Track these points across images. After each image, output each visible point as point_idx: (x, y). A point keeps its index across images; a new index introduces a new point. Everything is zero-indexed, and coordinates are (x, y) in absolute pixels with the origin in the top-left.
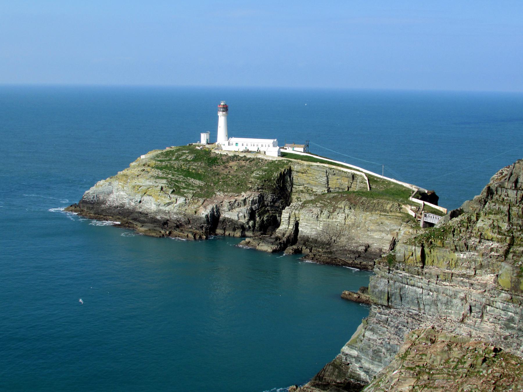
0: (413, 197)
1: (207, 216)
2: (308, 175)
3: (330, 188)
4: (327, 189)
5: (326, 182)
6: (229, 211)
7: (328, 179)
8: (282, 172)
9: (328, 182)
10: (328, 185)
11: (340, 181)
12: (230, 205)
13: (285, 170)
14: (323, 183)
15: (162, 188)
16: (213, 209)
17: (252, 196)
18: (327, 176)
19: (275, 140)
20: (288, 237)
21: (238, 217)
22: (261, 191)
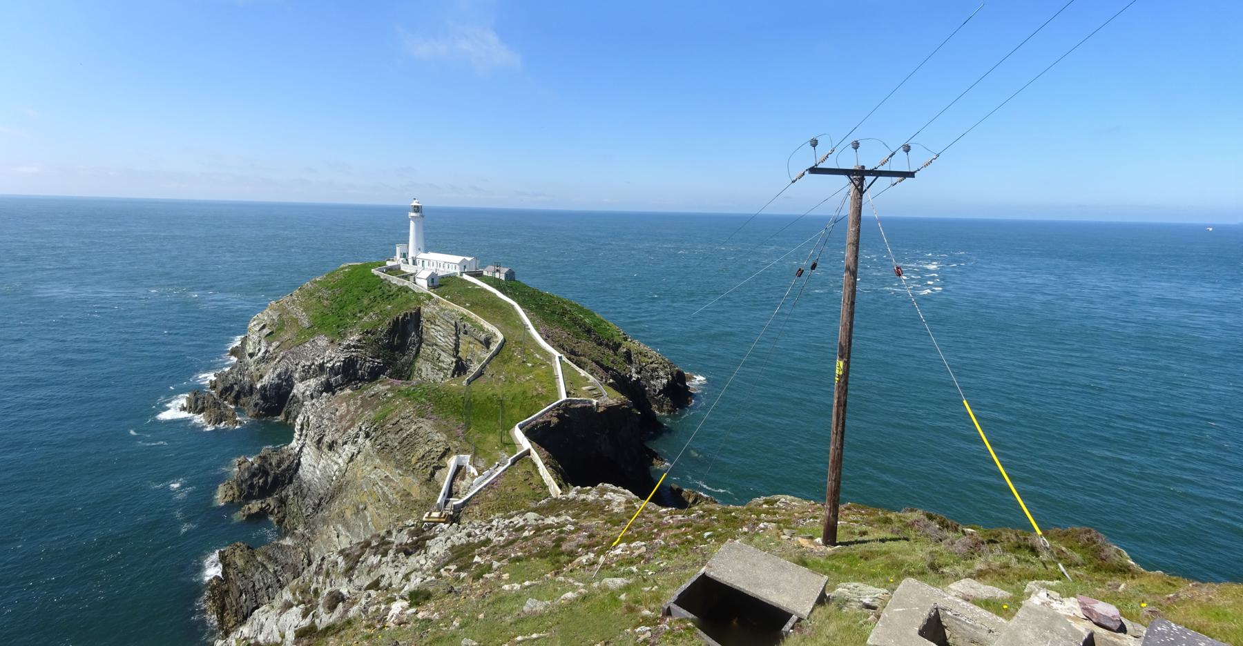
0: (521, 428)
1: (264, 388)
2: (436, 327)
3: (460, 359)
4: (454, 360)
5: (454, 346)
6: (302, 381)
7: (458, 338)
8: (400, 317)
9: (457, 345)
10: (458, 352)
11: (471, 346)
12: (304, 371)
13: (406, 315)
14: (450, 347)
15: (264, 327)
16: (279, 376)
17: (335, 360)
18: (456, 335)
19: (469, 259)
20: (283, 470)
21: (303, 397)
22: (353, 351)
